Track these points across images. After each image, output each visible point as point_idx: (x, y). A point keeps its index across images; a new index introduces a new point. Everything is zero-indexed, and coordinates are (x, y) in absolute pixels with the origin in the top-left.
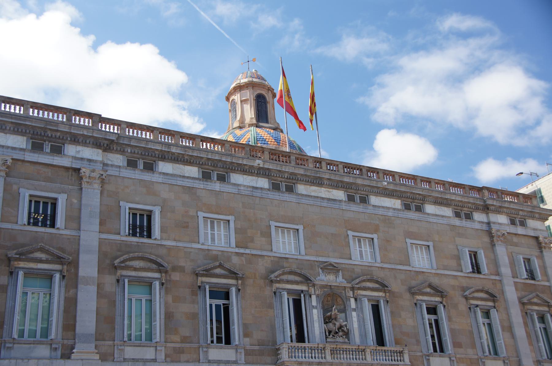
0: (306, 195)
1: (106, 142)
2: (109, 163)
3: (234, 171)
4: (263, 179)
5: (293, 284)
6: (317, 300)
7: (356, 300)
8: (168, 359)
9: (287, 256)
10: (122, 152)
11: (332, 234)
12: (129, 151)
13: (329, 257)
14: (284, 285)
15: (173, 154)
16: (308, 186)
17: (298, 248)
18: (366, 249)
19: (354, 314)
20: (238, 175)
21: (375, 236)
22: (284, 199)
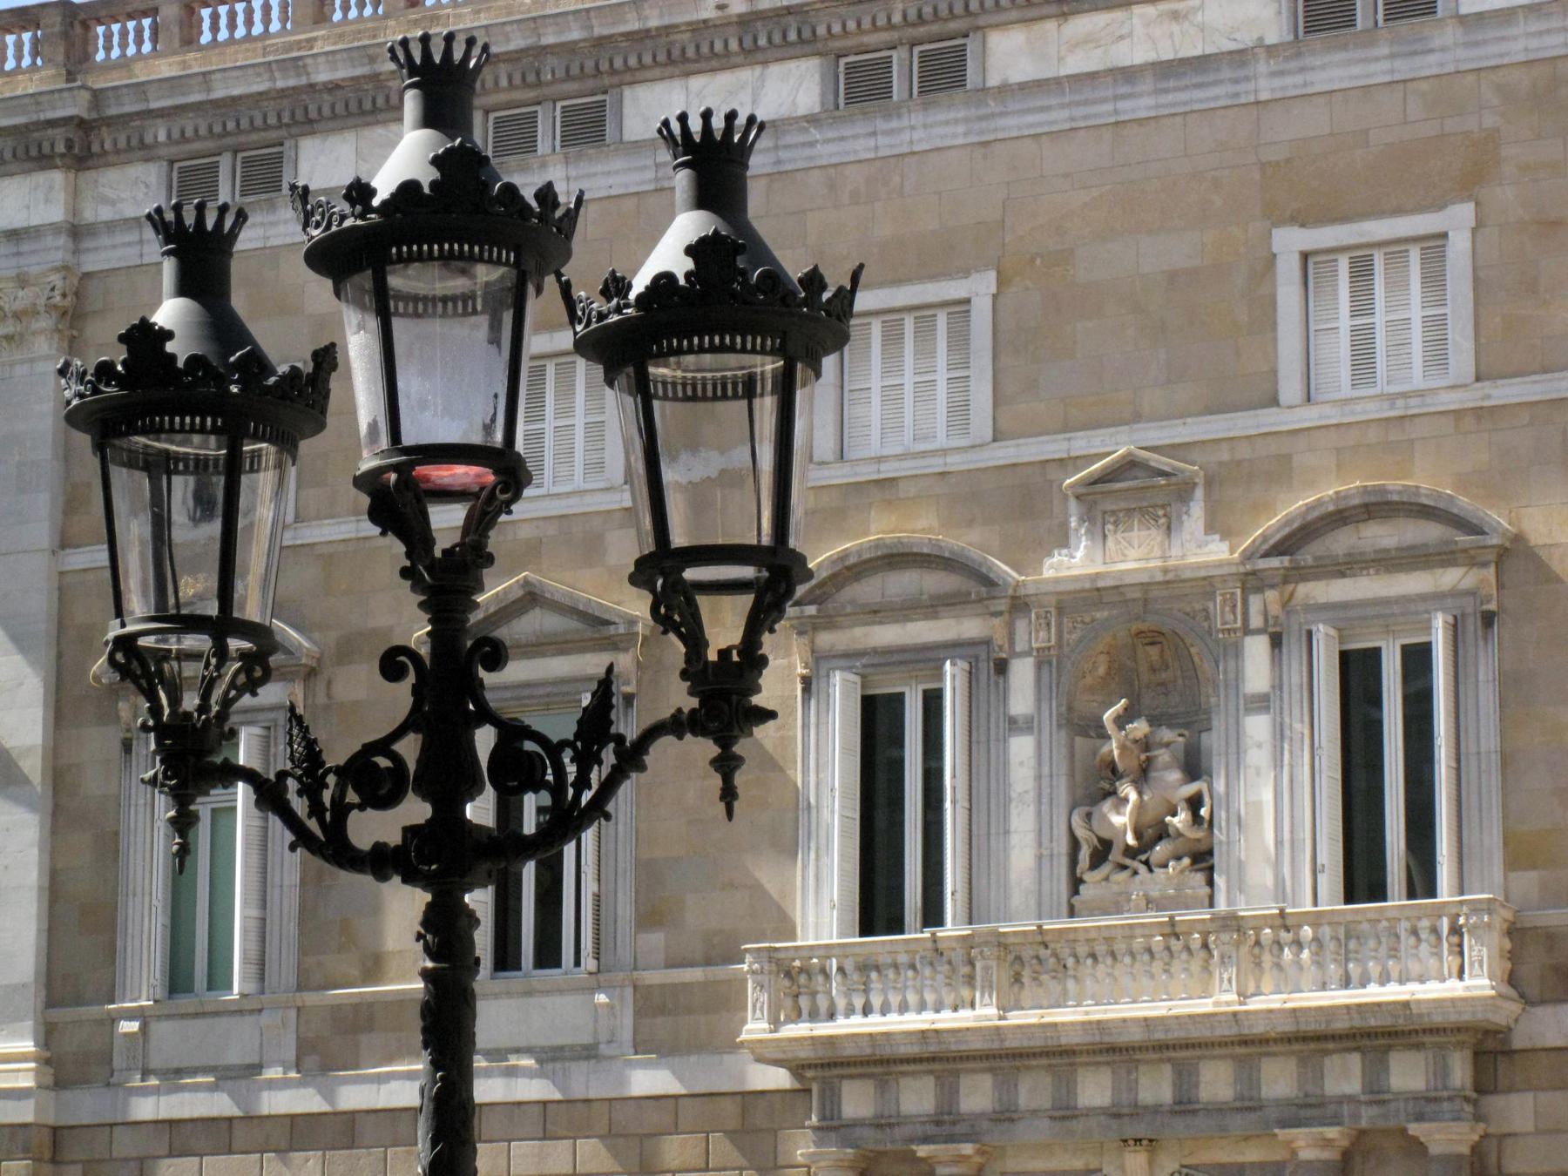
0: (1027, 88)
1: (59, 135)
2: (106, 214)
3: (634, 75)
4: (792, 65)
5: (907, 619)
6: (1038, 680)
7: (1276, 641)
8: (311, 1061)
9: (888, 470)
10: (143, 150)
11: (1173, 276)
12: (162, 137)
13: (1137, 418)
14: (858, 631)
15: (333, 87)
16: (1051, 25)
17: (960, 410)
18: (1403, 307)
19: (1257, 727)
20: (659, 88)
21: (1458, 219)
22: (901, 143)
